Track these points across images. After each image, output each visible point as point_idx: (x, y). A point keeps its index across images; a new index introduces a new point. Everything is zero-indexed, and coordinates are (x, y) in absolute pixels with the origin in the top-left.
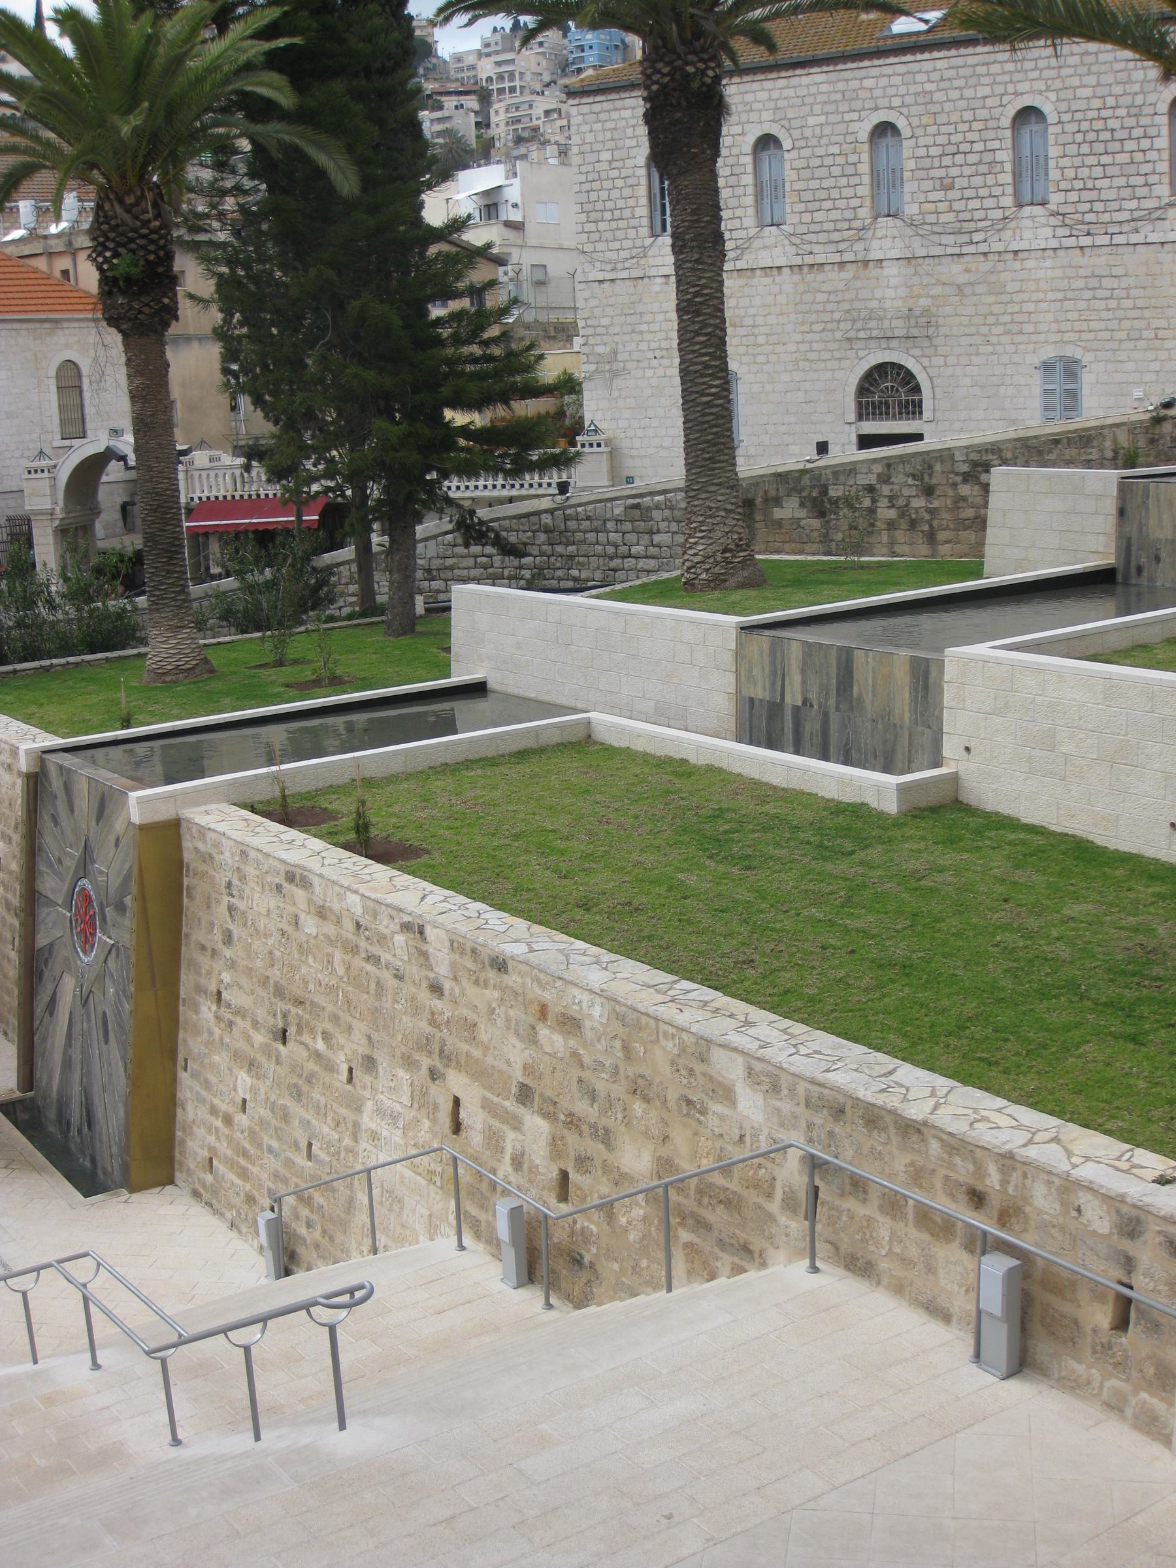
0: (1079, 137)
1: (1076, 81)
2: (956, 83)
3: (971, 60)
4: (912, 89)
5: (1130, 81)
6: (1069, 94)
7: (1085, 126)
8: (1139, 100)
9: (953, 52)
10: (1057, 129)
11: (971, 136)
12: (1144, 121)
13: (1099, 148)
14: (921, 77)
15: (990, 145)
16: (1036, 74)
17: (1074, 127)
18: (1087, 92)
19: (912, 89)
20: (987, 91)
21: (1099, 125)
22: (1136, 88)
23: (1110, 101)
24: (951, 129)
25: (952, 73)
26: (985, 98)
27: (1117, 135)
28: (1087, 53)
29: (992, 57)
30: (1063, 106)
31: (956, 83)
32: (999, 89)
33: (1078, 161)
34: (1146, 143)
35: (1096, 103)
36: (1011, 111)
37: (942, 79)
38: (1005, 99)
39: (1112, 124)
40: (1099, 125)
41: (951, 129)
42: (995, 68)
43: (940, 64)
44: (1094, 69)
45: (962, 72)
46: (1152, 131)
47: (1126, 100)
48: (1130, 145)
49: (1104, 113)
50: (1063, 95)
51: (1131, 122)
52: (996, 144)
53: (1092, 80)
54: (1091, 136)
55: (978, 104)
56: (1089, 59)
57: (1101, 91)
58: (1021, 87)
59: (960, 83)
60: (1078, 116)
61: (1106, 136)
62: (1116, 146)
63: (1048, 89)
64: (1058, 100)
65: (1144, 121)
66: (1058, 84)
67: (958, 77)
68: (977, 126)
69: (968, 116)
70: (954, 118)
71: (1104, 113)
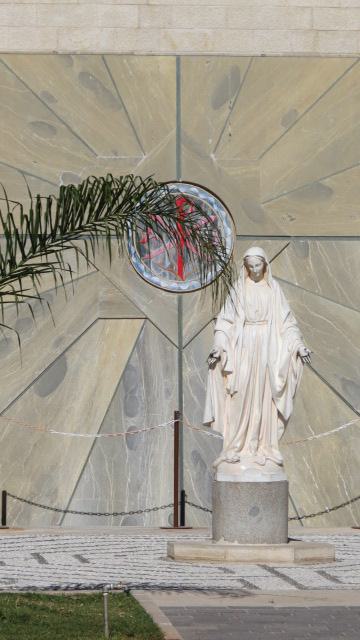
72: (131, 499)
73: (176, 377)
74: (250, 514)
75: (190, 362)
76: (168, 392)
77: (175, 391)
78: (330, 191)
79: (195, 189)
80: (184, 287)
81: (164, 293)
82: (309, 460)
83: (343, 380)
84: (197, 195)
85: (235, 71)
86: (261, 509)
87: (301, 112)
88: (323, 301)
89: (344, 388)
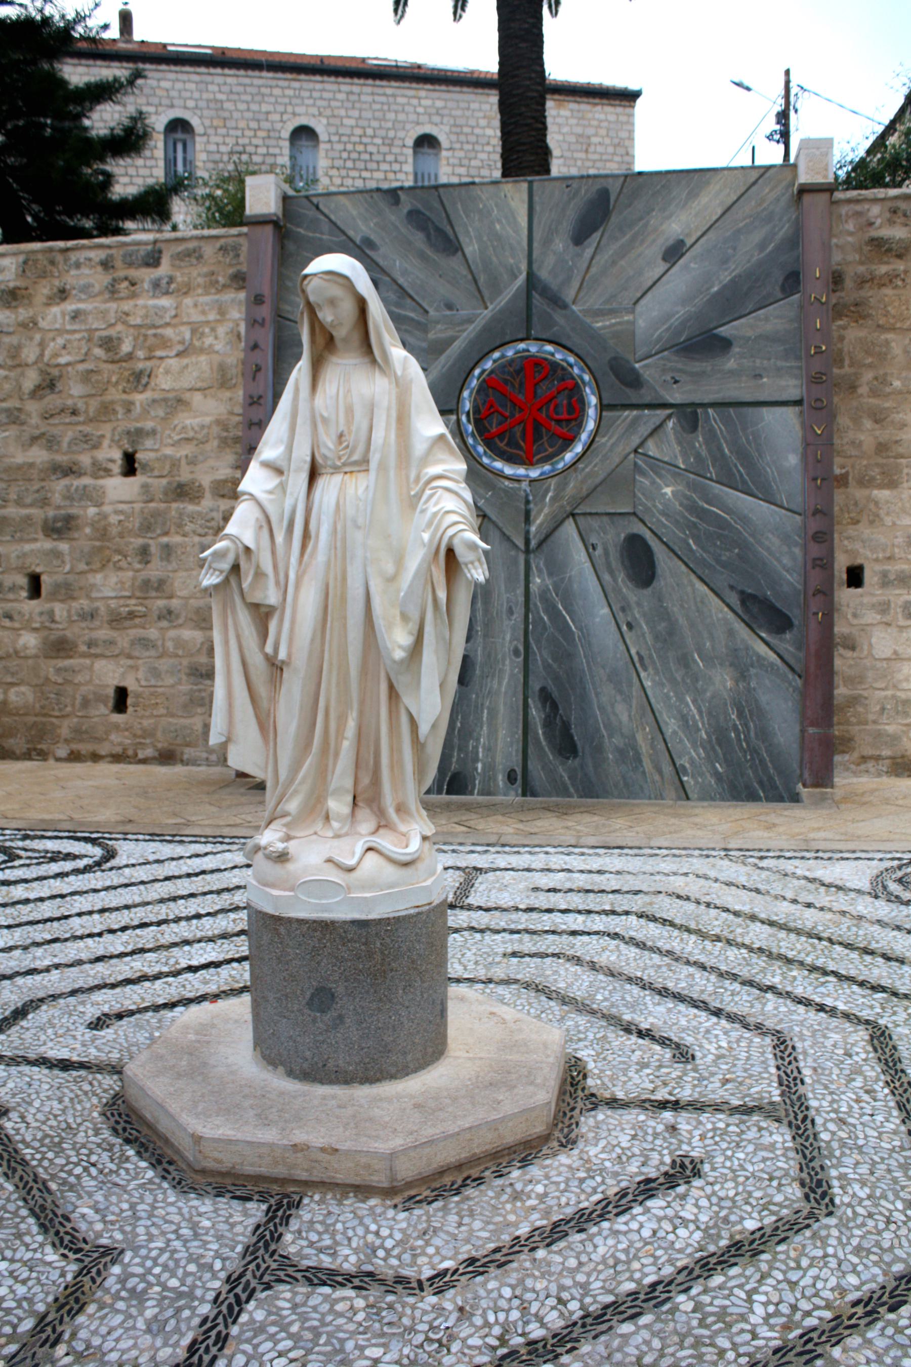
0: (345, 155)
1: (342, 112)
2: (244, 97)
3: (257, 82)
4: (205, 96)
5: (384, 120)
6: (337, 121)
7: (350, 147)
8: (391, 134)
9: (242, 72)
10: (328, 146)
11: (255, 141)
12: (395, 150)
13: (360, 165)
14: (211, 87)
15: (272, 151)
16: (311, 102)
17: (341, 147)
18: (352, 122)
19: (205, 96)
20: (271, 108)
21: (360, 148)
22: (390, 125)
23: (369, 132)
24: (239, 133)
25: (241, 89)
26: (268, 113)
27: (375, 157)
28: (352, 93)
29: (274, 83)
30: (332, 130)
31: (244, 97)
32: (281, 108)
33: (344, 173)
34: (396, 167)
35: (358, 132)
36: (290, 127)
37: (231, 92)
38: (285, 117)
39: (371, 149)
40: (360, 148)
41: (239, 133)
42: (277, 92)
43: (229, 80)
44: (357, 105)
45: (249, 89)
46: (401, 159)
47: (382, 133)
48: (384, 167)
49: (365, 140)
50: (332, 121)
51: (384, 149)
52: (277, 151)
53: (356, 114)
54: (354, 156)
55: (262, 117)
56: (353, 98)
57: (361, 123)
58: (298, 110)
59: (249, 98)
60: (344, 139)
61: (366, 157)
62: (374, 166)
63: (320, 114)
64: (329, 124)
65: (395, 150)
66: (328, 112)
67: (245, 93)
68: (261, 134)
69: (254, 125)
70: (242, 124)
71: (365, 140)
72: (460, 750)
73: (520, 591)
74: (310, 1004)
75: (539, 570)
76: (510, 611)
77: (519, 612)
78: (725, 344)
79: (549, 348)
80: (534, 473)
81: (507, 483)
82: (694, 701)
83: (742, 593)
84: (553, 355)
85: (603, 196)
86: (340, 990)
87: (689, 242)
88: (717, 488)
89: (743, 602)
